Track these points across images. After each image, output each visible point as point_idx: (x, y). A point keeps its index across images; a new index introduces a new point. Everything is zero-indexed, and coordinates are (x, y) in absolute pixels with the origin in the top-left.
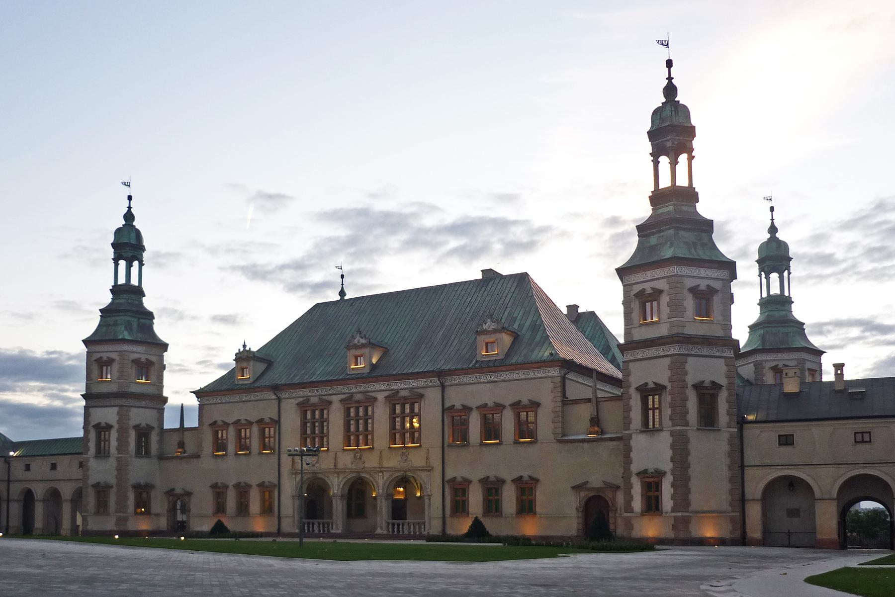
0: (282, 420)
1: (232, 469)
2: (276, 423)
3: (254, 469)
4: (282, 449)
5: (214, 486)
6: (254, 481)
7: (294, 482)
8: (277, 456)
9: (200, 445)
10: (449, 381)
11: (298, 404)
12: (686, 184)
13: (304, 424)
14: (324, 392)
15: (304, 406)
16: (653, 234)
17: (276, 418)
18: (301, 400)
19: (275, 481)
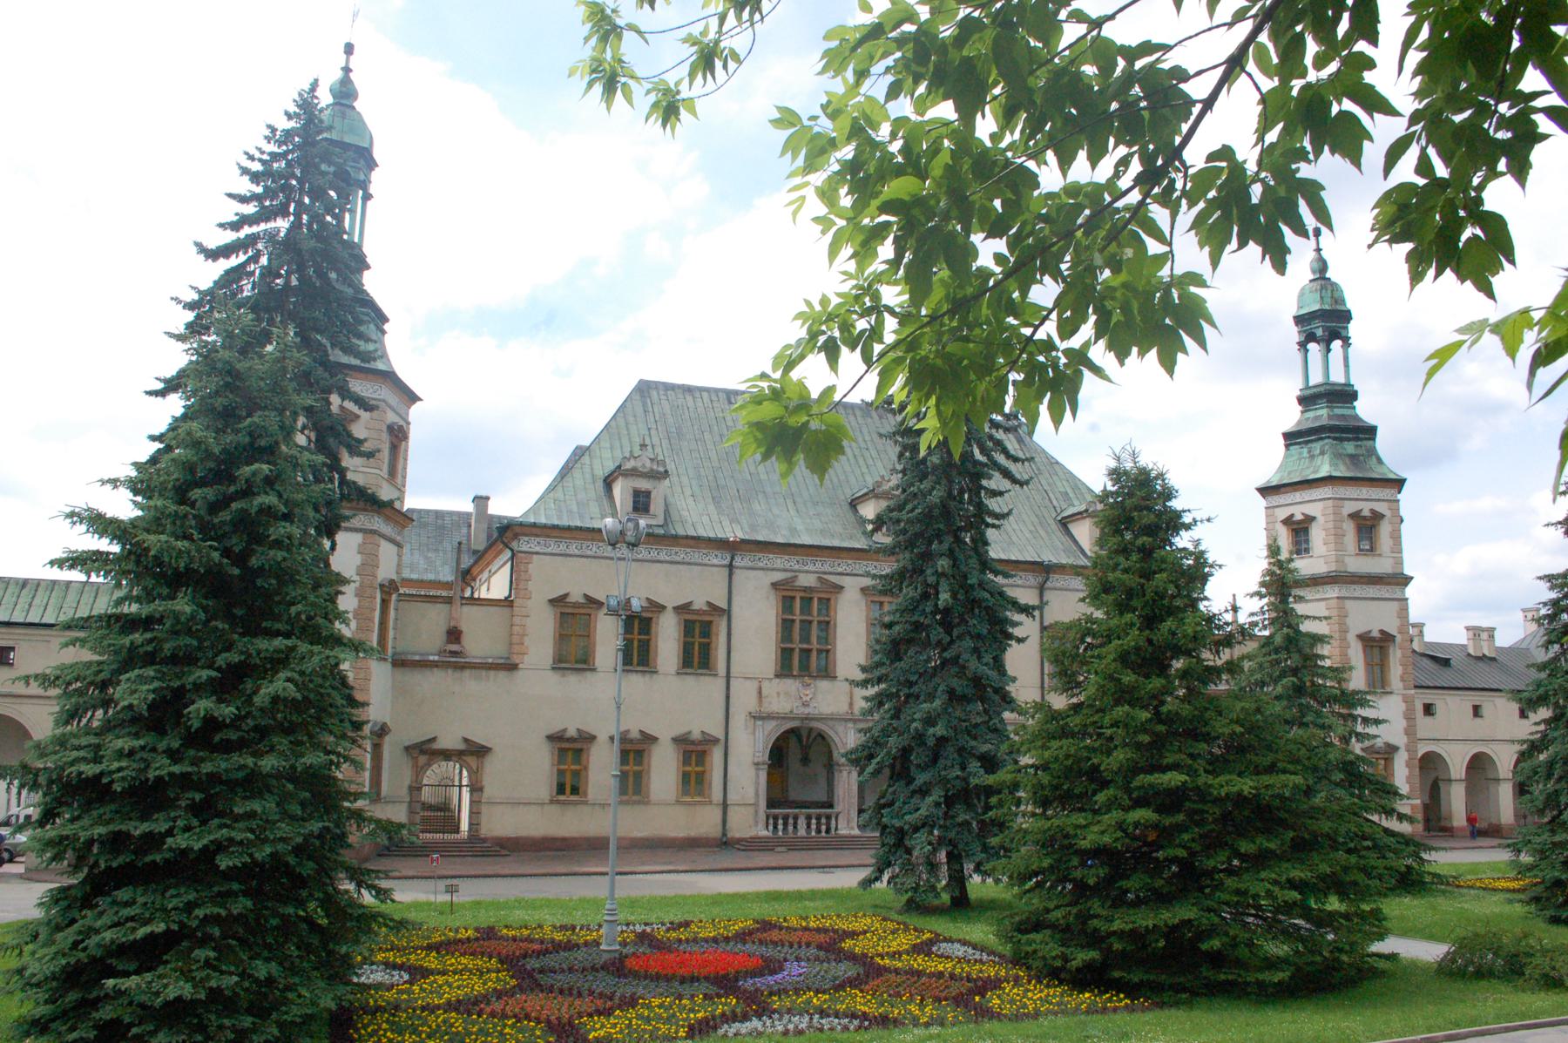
0: (735, 610)
1: (604, 700)
2: (727, 613)
3: (669, 703)
4: (734, 670)
5: (556, 738)
6: (665, 732)
7: (760, 735)
8: (721, 682)
9: (515, 640)
10: (1056, 580)
11: (775, 585)
12: (1342, 380)
13: (786, 626)
14: (827, 568)
15: (786, 594)
16: (1349, 440)
17: (723, 605)
18: (779, 576)
19: (718, 732)
